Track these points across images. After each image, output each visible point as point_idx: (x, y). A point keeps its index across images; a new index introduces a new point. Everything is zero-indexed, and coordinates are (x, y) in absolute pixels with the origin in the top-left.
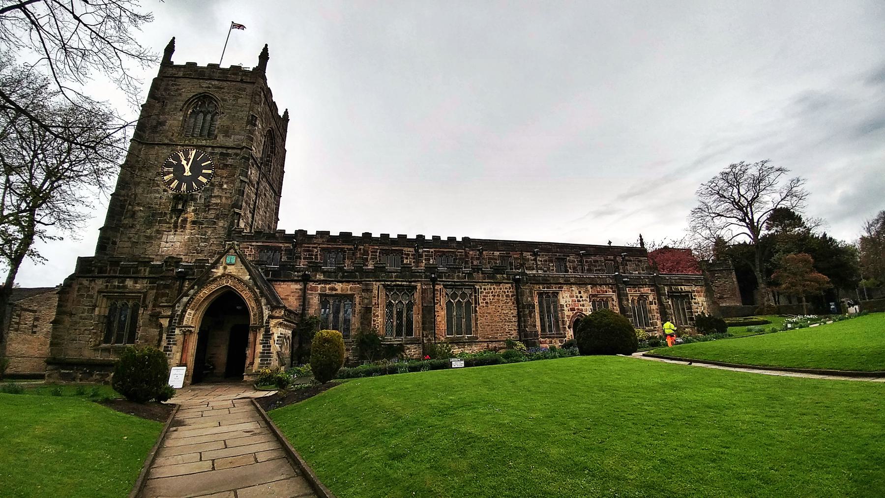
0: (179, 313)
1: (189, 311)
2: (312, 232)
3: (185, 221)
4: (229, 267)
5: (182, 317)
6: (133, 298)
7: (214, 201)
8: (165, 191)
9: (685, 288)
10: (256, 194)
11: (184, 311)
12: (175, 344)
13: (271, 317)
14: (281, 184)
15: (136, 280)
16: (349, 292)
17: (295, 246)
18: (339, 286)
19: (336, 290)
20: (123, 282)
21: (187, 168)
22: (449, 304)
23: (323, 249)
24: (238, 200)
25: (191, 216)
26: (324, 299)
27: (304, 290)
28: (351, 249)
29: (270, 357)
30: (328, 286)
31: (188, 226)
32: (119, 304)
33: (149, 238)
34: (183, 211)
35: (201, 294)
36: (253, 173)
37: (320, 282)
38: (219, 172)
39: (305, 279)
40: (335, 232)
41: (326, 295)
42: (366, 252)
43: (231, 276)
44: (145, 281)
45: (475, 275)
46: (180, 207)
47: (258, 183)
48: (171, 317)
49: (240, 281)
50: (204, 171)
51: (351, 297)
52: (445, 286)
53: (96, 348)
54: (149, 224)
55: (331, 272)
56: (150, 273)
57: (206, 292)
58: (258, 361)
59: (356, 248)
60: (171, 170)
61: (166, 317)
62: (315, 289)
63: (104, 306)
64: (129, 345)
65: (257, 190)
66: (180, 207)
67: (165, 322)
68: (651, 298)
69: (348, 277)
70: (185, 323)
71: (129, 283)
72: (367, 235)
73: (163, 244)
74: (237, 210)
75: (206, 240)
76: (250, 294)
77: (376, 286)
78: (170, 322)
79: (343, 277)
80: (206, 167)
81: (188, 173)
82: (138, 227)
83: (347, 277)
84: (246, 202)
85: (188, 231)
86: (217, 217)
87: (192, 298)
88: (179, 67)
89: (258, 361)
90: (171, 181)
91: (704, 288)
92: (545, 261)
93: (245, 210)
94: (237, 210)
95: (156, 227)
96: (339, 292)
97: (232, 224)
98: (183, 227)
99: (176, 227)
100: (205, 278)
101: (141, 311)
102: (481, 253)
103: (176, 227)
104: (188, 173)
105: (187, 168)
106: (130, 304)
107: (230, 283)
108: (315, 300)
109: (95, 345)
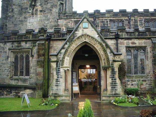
0: (61, 59)
1: (66, 58)
2: (103, 11)
3: (37, 10)
4: (85, 30)
5: (63, 61)
6: (25, 52)
11: (64, 58)
12: (61, 78)
13: (114, 61)
15: (26, 42)
16: (143, 45)
19: (135, 44)
20: (20, 43)
23: (111, 20)
25: (39, 8)
26: (128, 49)
27: (117, 44)
28: (127, 20)
29: (116, 86)
30: (130, 41)
31: (39, 13)
32: (19, 56)
33: (22, 21)
34: (35, 5)
35: (71, 47)
39: (117, 37)
40: (116, 10)
41: (129, 47)
42: (136, 21)
43: (88, 35)
44: (30, 42)
46: (33, 3)
48: (57, 62)
49: (93, 38)
53: (11, 78)
54: (21, 14)
55: (131, 33)
56: (32, 37)
58: (109, 88)
59: (130, 19)
61: (54, 62)
63: (12, 56)
64: (27, 77)
66: (33, 3)
67: (54, 65)
70: (65, 65)
71: (23, 44)
72: (135, 11)
73: (28, 24)
75: (48, 20)
76: (100, 47)
78: (57, 65)
79: (139, 35)
82: (16, 16)
83: (142, 35)
85: (39, 16)
86: (52, 7)
87: (67, 50)
89: (109, 88)
95: (24, 15)
96: (137, 45)
97: (60, 9)
98: (36, 14)
99: (33, 14)
100: (72, 37)
101: (31, 58)
103: (33, 14)
106: (24, 55)
107: (87, 40)
108: (123, 50)
109: (11, 77)
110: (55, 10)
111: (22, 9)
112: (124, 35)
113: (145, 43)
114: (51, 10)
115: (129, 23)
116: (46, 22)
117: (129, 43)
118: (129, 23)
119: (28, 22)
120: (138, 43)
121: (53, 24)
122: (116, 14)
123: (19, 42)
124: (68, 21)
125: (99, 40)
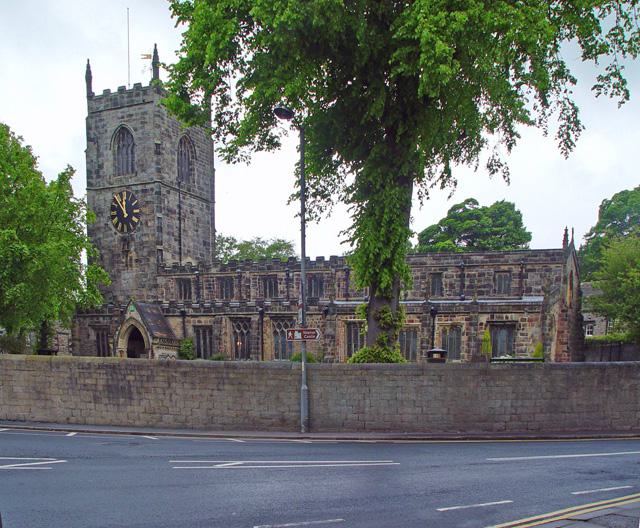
3: (131, 259)
7: (145, 239)
8: (116, 234)
9: (513, 317)
10: (179, 219)
14: (213, 186)
16: (209, 324)
18: (203, 319)
21: (124, 210)
22: (275, 333)
24: (158, 237)
25: (133, 255)
26: (196, 328)
27: (184, 322)
30: (197, 319)
31: (134, 264)
36: (172, 200)
37: (192, 316)
38: (144, 210)
39: (183, 315)
45: (293, 307)
47: (179, 207)
50: (135, 211)
51: (209, 329)
52: (271, 318)
57: (125, 328)
60: (115, 213)
62: (189, 322)
65: (180, 214)
68: (464, 329)
71: (101, 319)
74: (159, 247)
75: (146, 276)
77: (225, 318)
80: (136, 207)
81: (126, 215)
84: (168, 234)
90: (117, 224)
91: (540, 316)
92: (417, 278)
93: (169, 240)
94: (159, 247)
98: (131, 266)
103: (127, 265)
104: (126, 215)
105: (124, 210)
107: (133, 323)
108: (190, 331)
110: (153, 260)
111: (113, 256)
112: (191, 312)
114: (148, 260)
116: (144, 280)
119: (123, 277)
120: (205, 321)
121: (152, 283)
122: (223, 269)
123: (98, 317)
124: (167, 279)
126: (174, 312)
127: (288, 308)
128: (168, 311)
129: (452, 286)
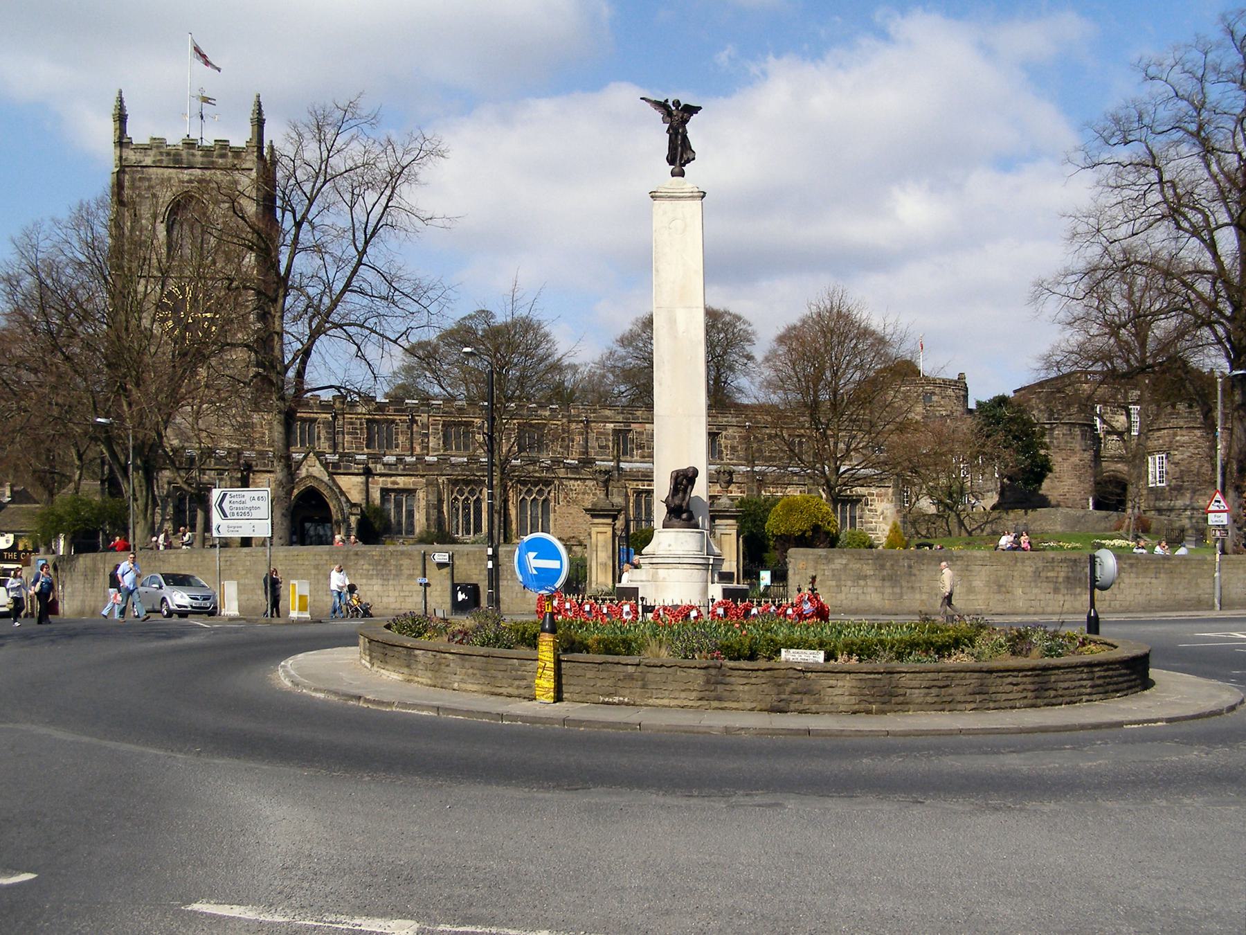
16: (411, 487)
17: (335, 418)
23: (368, 421)
26: (385, 492)
28: (404, 421)
30: (389, 480)
37: (381, 475)
39: (368, 473)
51: (411, 492)
69: (409, 471)
88: (145, 149)
96: (401, 486)
102: (587, 426)
108: (376, 495)
112: (379, 468)
113: (414, 483)
115: (410, 427)
117: (388, 482)
118: (410, 427)
120: (402, 482)
125: (330, 483)
126: (349, 467)
127: (548, 469)
128: (336, 465)
129: (733, 448)
